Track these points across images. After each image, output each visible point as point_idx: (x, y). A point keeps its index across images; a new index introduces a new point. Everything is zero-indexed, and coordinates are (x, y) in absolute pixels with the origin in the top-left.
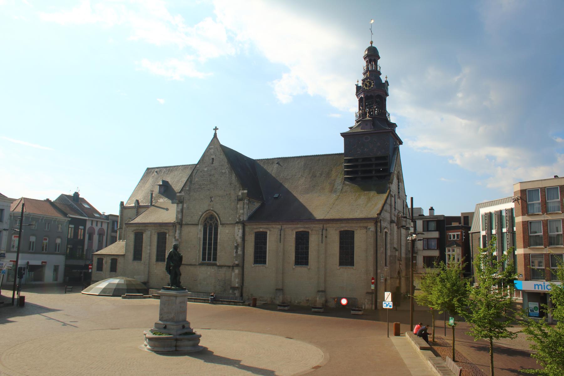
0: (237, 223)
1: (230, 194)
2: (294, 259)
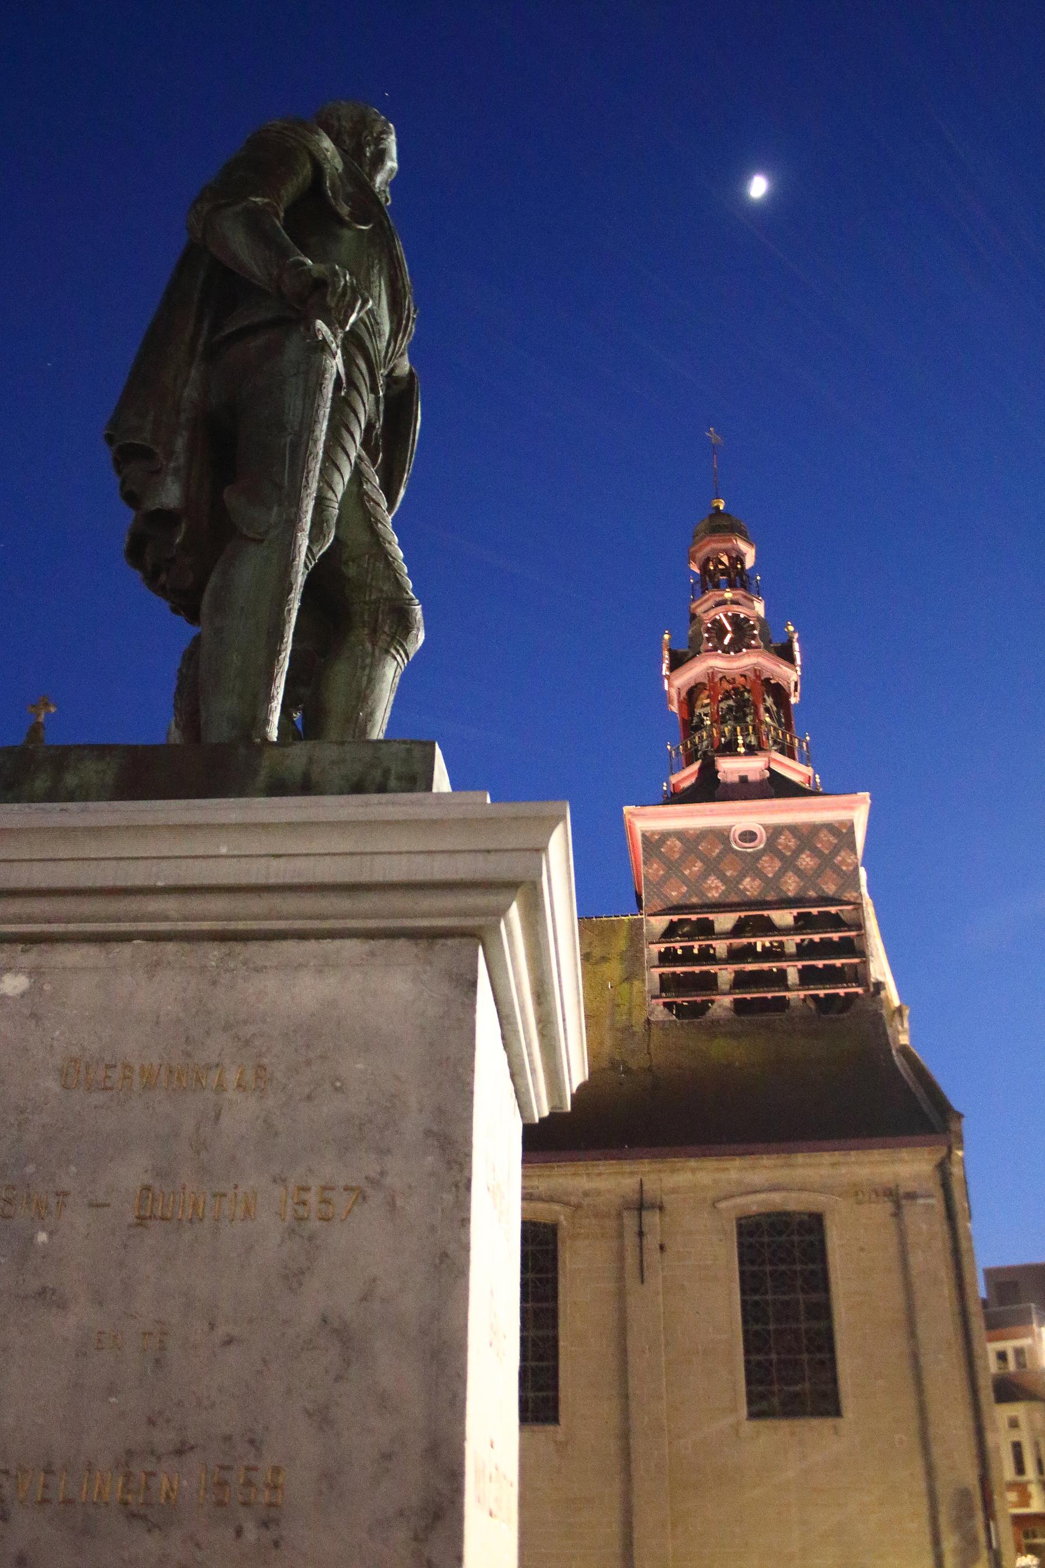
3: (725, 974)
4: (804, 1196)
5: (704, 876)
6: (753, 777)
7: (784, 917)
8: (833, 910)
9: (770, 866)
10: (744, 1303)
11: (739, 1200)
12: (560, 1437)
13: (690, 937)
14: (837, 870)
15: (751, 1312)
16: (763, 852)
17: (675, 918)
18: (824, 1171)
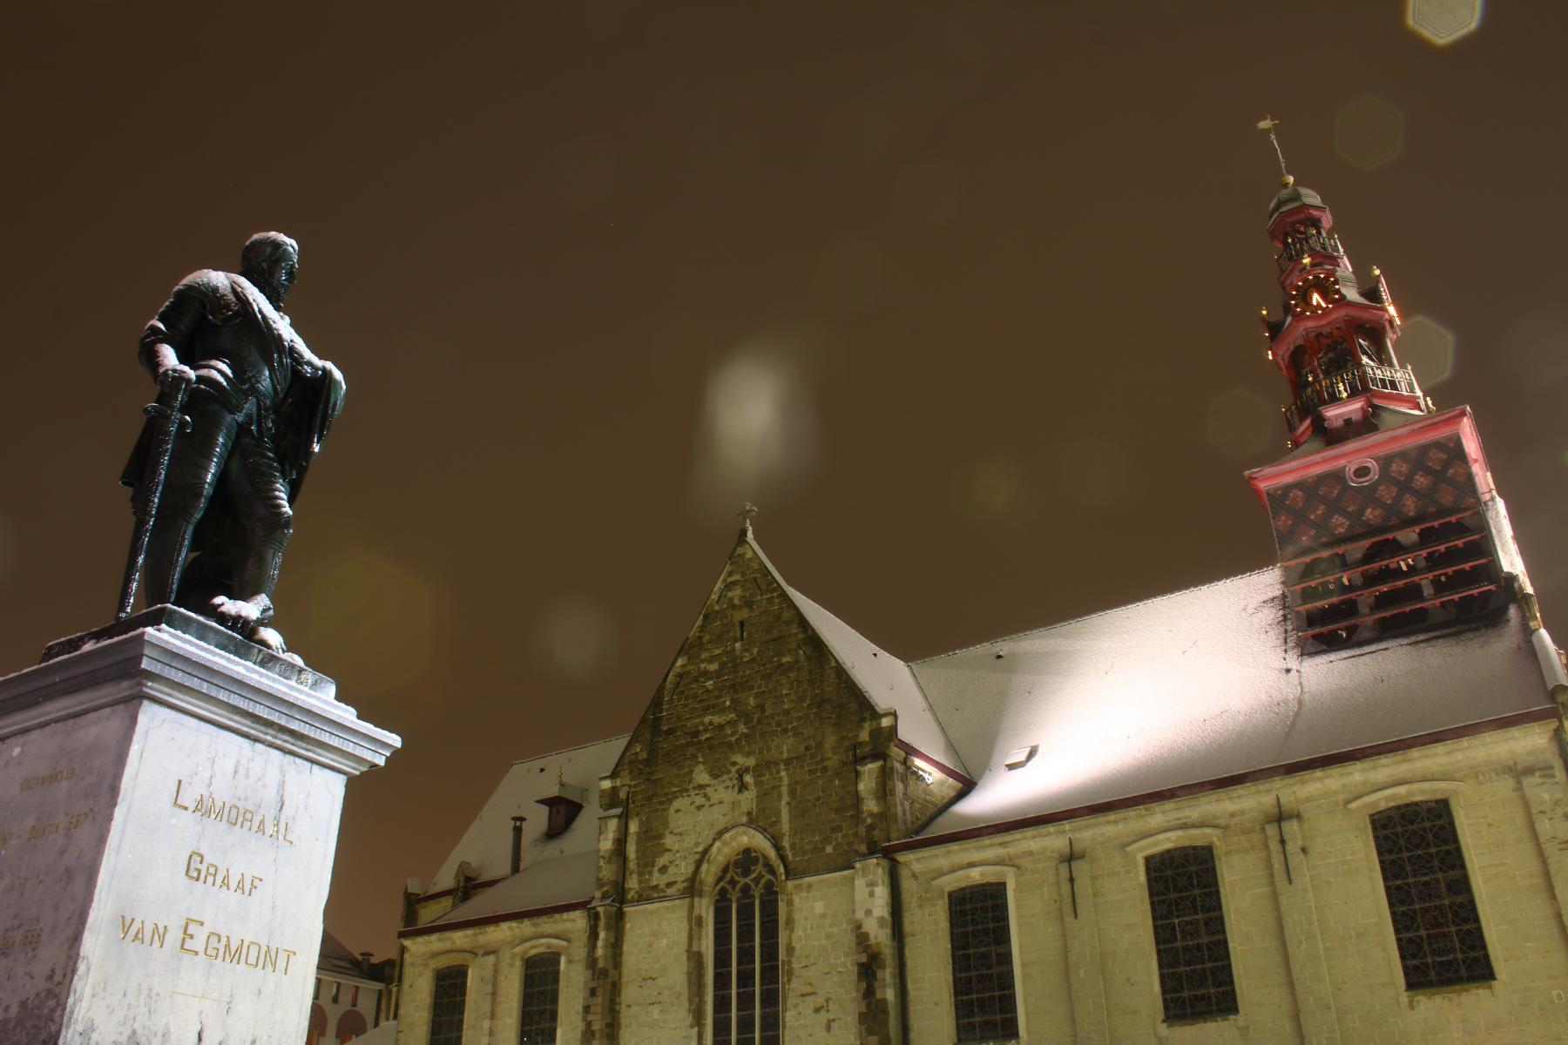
1: (820, 745)
2: (1157, 988)
4: (1427, 785)
5: (1328, 516)
6: (1356, 417)
7: (1409, 536)
8: (1453, 519)
10: (1387, 888)
11: (1366, 799)
12: (1241, 1023)
13: (1324, 574)
15: (1396, 896)
17: (1308, 559)
18: (1442, 760)
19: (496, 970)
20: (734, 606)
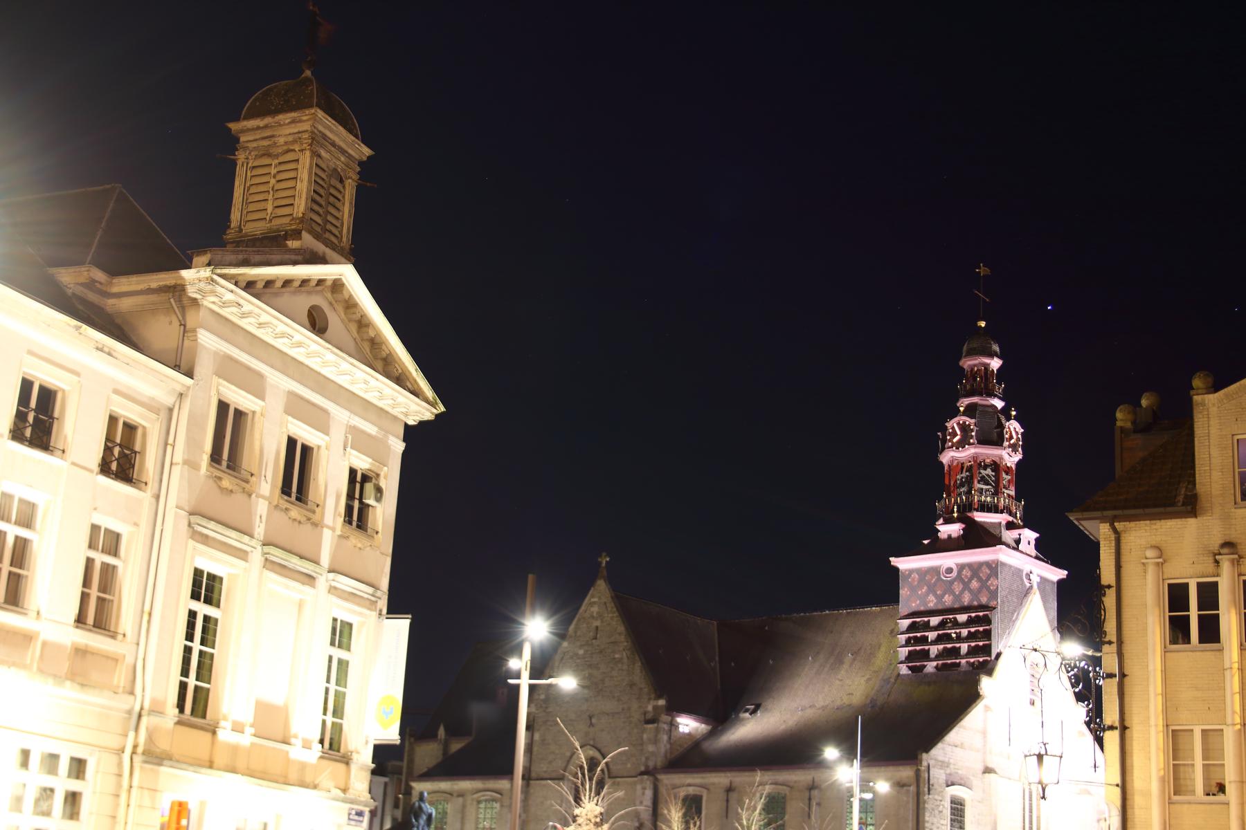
0: (642, 773)
1: (629, 709)
3: (934, 650)
5: (927, 594)
6: (954, 535)
7: (962, 618)
9: (957, 587)
14: (988, 588)
16: (955, 580)
19: (464, 806)
20: (593, 617)
